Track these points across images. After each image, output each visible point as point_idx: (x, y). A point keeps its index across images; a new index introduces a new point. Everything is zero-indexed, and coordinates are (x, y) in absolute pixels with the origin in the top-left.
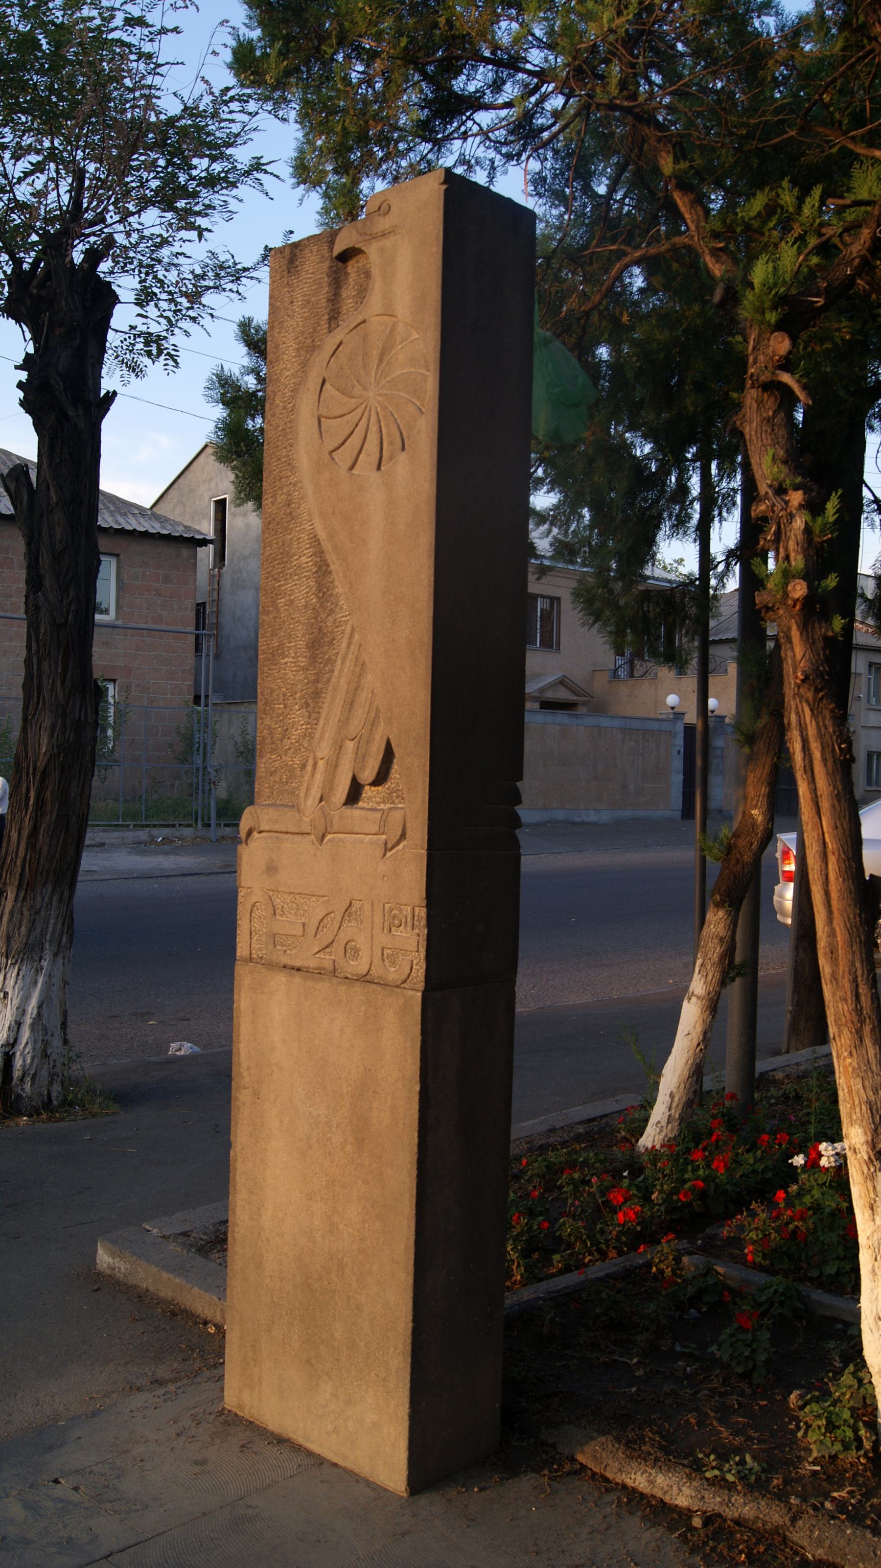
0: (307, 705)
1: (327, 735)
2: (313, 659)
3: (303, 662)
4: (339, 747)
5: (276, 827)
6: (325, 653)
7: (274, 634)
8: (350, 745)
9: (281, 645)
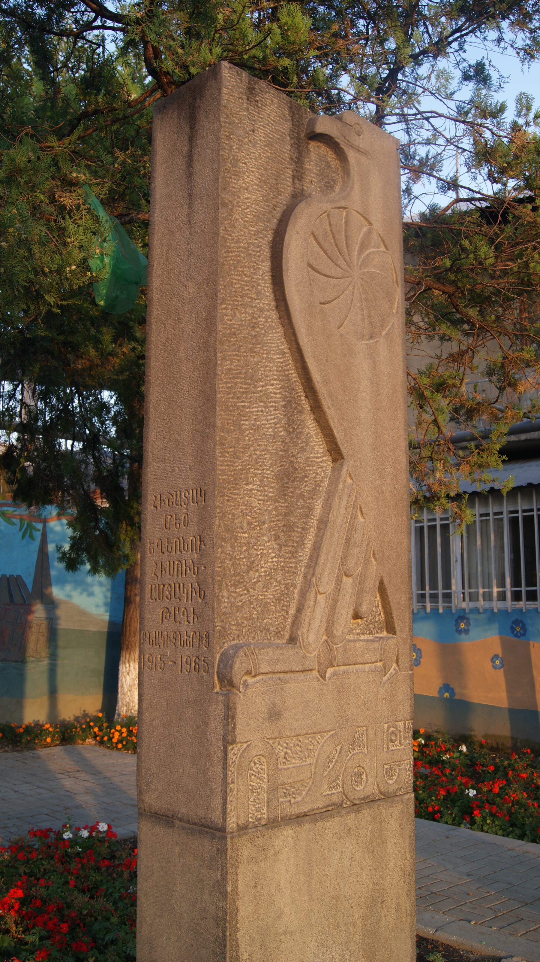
0: (277, 537)
1: (327, 571)
2: (283, 490)
3: (271, 492)
4: (339, 581)
5: (278, 667)
6: (295, 488)
7: (235, 456)
8: (348, 582)
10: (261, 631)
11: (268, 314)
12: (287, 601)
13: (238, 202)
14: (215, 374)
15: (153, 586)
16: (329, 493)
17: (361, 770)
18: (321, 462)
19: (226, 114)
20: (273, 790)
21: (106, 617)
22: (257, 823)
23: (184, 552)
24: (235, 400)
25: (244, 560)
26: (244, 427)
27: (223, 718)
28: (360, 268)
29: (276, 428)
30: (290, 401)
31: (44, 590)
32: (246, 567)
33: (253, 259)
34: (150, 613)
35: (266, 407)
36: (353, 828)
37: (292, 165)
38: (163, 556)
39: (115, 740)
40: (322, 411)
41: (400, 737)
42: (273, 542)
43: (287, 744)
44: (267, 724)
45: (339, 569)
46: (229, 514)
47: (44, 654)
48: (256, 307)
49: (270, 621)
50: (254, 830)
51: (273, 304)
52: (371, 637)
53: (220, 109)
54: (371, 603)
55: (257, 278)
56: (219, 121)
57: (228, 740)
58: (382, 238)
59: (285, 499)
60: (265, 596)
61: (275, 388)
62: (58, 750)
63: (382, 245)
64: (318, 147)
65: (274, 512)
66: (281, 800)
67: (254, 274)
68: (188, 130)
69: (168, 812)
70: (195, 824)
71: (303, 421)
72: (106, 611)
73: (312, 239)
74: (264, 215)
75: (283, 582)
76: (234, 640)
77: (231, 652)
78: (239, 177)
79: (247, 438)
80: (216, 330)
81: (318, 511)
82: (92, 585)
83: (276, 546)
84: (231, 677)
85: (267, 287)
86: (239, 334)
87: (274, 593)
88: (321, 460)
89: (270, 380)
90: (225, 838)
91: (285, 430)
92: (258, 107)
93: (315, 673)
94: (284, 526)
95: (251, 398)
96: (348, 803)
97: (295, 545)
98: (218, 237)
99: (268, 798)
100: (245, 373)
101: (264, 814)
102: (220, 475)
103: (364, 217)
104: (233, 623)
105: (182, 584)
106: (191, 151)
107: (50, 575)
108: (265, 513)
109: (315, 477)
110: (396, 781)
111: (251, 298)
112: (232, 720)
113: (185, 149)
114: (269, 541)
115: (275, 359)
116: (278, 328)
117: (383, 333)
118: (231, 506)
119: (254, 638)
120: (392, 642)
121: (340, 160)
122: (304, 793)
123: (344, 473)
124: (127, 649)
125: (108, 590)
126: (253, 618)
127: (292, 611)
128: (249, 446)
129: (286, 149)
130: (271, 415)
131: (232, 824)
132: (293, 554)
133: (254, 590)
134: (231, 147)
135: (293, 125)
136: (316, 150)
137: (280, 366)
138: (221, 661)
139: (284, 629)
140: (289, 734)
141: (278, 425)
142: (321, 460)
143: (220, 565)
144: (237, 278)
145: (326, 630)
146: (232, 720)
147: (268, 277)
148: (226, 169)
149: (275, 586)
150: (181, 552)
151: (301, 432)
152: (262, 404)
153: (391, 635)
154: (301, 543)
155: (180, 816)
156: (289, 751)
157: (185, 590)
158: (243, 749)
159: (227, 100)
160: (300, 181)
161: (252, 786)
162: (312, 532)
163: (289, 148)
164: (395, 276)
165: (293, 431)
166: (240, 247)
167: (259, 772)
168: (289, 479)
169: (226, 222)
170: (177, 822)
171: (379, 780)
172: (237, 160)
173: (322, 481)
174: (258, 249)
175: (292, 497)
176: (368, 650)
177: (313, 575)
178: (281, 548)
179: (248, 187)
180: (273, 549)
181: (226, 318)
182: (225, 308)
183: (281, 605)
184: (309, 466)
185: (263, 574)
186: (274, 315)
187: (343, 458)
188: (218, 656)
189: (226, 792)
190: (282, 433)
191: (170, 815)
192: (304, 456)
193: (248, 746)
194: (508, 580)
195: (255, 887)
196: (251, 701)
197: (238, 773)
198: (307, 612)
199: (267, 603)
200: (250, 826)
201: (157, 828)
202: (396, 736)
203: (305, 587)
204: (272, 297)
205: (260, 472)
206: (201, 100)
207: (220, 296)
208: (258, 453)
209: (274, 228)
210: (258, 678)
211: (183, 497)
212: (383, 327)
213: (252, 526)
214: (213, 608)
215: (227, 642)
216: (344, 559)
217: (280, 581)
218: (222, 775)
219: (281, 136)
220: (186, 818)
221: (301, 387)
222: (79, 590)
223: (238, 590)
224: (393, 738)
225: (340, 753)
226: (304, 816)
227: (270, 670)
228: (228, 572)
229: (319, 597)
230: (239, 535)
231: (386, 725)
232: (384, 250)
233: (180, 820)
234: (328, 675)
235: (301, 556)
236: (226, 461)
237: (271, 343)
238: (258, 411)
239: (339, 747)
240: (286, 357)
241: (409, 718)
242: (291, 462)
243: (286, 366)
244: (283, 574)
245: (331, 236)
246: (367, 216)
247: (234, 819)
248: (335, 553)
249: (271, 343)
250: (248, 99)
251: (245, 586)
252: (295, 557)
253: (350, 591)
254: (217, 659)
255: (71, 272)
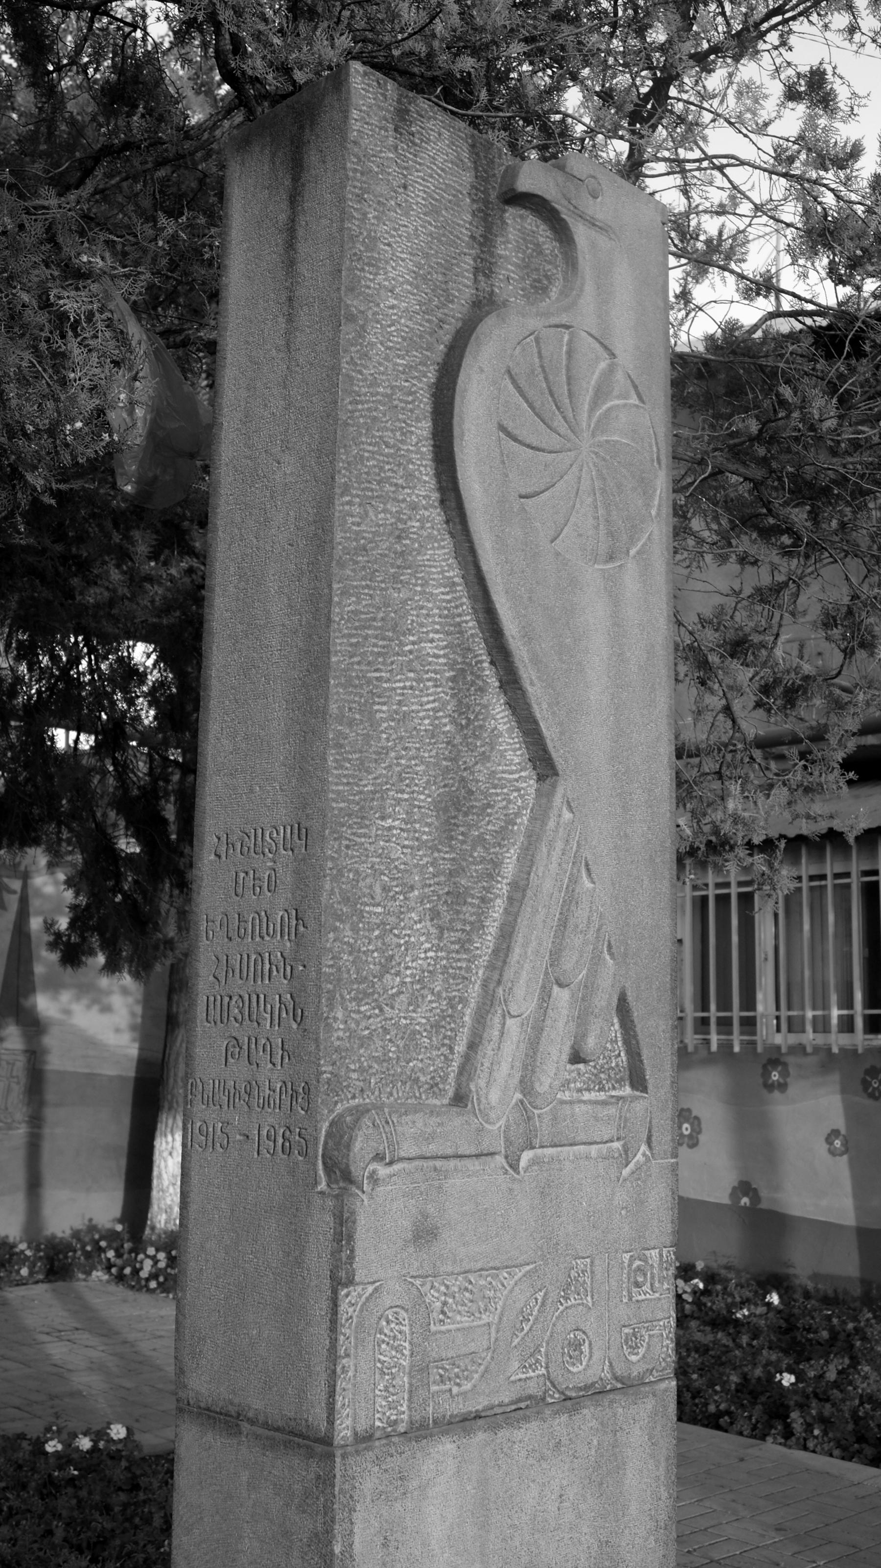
0: (435, 914)
1: (524, 975)
2: (448, 830)
4: (545, 996)
5: (432, 1148)
6: (470, 826)
7: (362, 766)
8: (562, 996)
9: (379, 793)
10: (404, 1083)
11: (427, 513)
12: (451, 1030)
13: (374, 314)
14: (329, 619)
15: (212, 999)
16: (530, 836)
17: (580, 1336)
18: (517, 780)
19: (355, 156)
20: (420, 1370)
21: (133, 1051)
22: (389, 1429)
23: (267, 938)
24: (364, 668)
25: (376, 954)
26: (378, 715)
27: (331, 1238)
28: (593, 435)
29: (437, 718)
30: (463, 671)
31: (22, 1000)
32: (378, 967)
33: (400, 416)
34: (205, 1047)
35: (419, 680)
36: (565, 1440)
37: (473, 248)
38: (230, 944)
39: (144, 1274)
40: (521, 688)
41: (652, 1278)
42: (429, 923)
43: (447, 1287)
44: (411, 1250)
45: (546, 973)
46: (350, 871)
47: (19, 1116)
48: (404, 500)
49: (420, 1065)
50: (384, 1441)
51: (435, 496)
52: (602, 1096)
53: (345, 148)
54: (604, 1036)
55: (408, 450)
56: (344, 168)
57: (340, 1278)
58: (632, 381)
59: (450, 846)
60: (412, 1019)
61: (436, 647)
62: (41, 1291)
63: (633, 392)
64: (521, 217)
65: (431, 869)
66: (434, 1388)
67: (402, 442)
68: (288, 182)
69: (230, 1408)
70: (277, 1429)
71: (485, 707)
72: (134, 1040)
73: (508, 382)
74: (421, 337)
75: (444, 995)
76: (354, 1097)
77: (348, 1119)
78: (378, 268)
79: (384, 736)
80: (331, 541)
81: (509, 868)
82: (109, 993)
83: (433, 930)
84: (348, 1165)
85: (426, 466)
86: (373, 549)
87: (428, 1014)
88: (516, 776)
89: (427, 633)
90: (331, 1456)
91: (453, 721)
92: (416, 145)
93: (500, 1160)
94: (448, 893)
95: (392, 663)
96: (557, 1396)
97: (468, 928)
98: (338, 374)
99: (411, 1385)
100: (383, 619)
101: (403, 1414)
102: (334, 800)
103: (601, 343)
104: (352, 1067)
105: (262, 996)
106: (293, 221)
107: (32, 973)
108: (415, 871)
109: (505, 808)
110: (644, 1356)
111: (396, 485)
112: (348, 1243)
113: (283, 217)
114: (420, 921)
115: (437, 595)
116: (443, 540)
117: (633, 552)
118: (353, 857)
119: (391, 1094)
120: (640, 1106)
121: (561, 241)
122: (476, 1376)
123: (558, 800)
124: (170, 1109)
125: (137, 1002)
126: (390, 1058)
127: (460, 1048)
128: (388, 750)
129: (464, 220)
130: (428, 695)
131: (344, 1430)
132: (464, 945)
133: (393, 1008)
134: (365, 214)
135: (476, 177)
136: (518, 224)
137: (445, 608)
138: (329, 1135)
139: (444, 1079)
140: (450, 1269)
141: (441, 714)
142: (516, 776)
143: (331, 963)
144: (371, 448)
145: (521, 1082)
146: (348, 1243)
147: (426, 449)
148: (355, 254)
149: (430, 1002)
150: (262, 938)
151: (481, 727)
152: (412, 675)
153: (638, 1093)
154: (479, 926)
155: (251, 1414)
156: (450, 1301)
157: (269, 1006)
158: (367, 1294)
159: (359, 131)
160: (487, 276)
161: (383, 1362)
162: (500, 904)
163: (468, 217)
164: (655, 449)
165: (468, 725)
166: (378, 393)
167: (395, 1337)
168: (459, 810)
169: (353, 349)
170: (245, 1426)
171: (612, 1354)
172: (375, 239)
173: (518, 814)
174: (410, 398)
175: (463, 842)
176: (596, 1119)
177: (499, 982)
178: (442, 933)
179: (394, 287)
180: (428, 934)
181: (350, 520)
182: (349, 503)
183: (441, 1037)
184: (495, 787)
185: (408, 980)
186: (437, 516)
187: (557, 774)
188: (325, 1127)
189: (334, 1372)
190: (448, 728)
191: (233, 1413)
192: (488, 769)
193: (376, 1290)
194: (858, 996)
195: (385, 1545)
196: (383, 1209)
197: (356, 1338)
198: (488, 1049)
199: (414, 1032)
200: (378, 1434)
201: (209, 1437)
202: (645, 1275)
203: (484, 1004)
204: (432, 483)
205: (406, 796)
206: (312, 131)
207: (340, 480)
208: (403, 762)
209: (440, 360)
210: (397, 1167)
211: (268, 838)
212: (632, 541)
213: (391, 894)
214: (317, 1040)
215: (342, 1101)
216: (555, 956)
217: (439, 993)
218: (327, 1342)
219: (454, 196)
220: (261, 1418)
221: (483, 645)
222: (85, 1001)
223: (363, 1009)
224: (640, 1279)
225: (543, 1304)
226: (475, 1418)
227: (419, 1153)
228: (345, 976)
229: (509, 1022)
230: (367, 909)
231: (627, 1256)
232: (637, 402)
233: (252, 1422)
234: (523, 1163)
235: (477, 948)
236: (345, 776)
237: (430, 566)
238: (404, 688)
239: (542, 1294)
240: (456, 591)
241: (668, 1244)
242: (463, 779)
243: (457, 607)
244: (445, 981)
245: (541, 377)
246: (606, 342)
247: (349, 1422)
248: (540, 944)
249: (430, 566)
250: (396, 130)
251: (376, 1000)
252: (467, 951)
253: (565, 1012)
254: (323, 1132)
255: (74, 432)
